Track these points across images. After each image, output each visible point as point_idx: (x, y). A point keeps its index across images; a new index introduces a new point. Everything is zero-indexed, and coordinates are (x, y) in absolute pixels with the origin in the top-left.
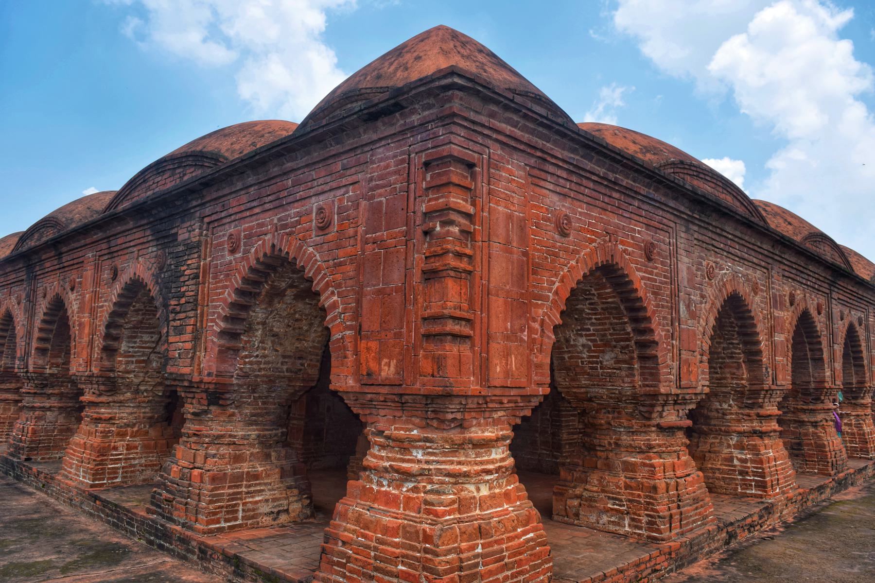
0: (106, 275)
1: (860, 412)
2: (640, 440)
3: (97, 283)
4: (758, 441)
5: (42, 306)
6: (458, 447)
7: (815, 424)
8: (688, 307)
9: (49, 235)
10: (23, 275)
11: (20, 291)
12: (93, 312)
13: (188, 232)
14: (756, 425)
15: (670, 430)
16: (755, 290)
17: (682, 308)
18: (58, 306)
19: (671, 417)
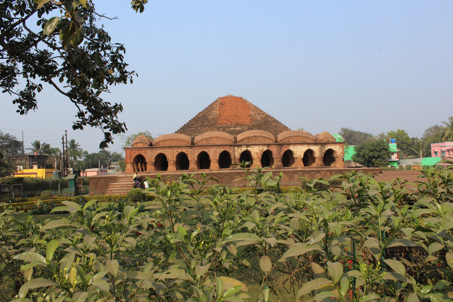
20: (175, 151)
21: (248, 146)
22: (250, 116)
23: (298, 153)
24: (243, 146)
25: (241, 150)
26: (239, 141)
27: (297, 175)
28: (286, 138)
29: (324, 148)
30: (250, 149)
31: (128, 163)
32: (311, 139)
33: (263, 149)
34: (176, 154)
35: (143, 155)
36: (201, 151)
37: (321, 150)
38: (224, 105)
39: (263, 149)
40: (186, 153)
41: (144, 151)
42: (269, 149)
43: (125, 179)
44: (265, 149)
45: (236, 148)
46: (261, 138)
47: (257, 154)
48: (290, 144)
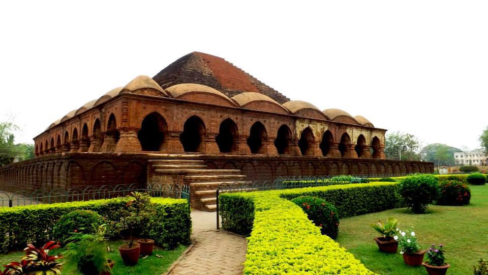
1: (268, 143)
3: (92, 119)
4: (207, 143)
5: (83, 125)
6: (127, 134)
8: (176, 118)
10: (78, 120)
11: (79, 123)
12: (92, 124)
13: (103, 110)
14: (208, 140)
15: (173, 137)
16: (204, 114)
17: (175, 118)
18: (86, 125)
19: (173, 134)
20: (219, 114)
21: (311, 121)
22: (253, 84)
24: (306, 121)
25: (303, 126)
26: (295, 113)
28: (337, 117)
29: (372, 135)
30: (311, 126)
31: (130, 129)
32: (357, 123)
33: (324, 128)
34: (220, 121)
35: (163, 114)
36: (255, 120)
37: (370, 138)
38: (210, 63)
39: (324, 128)
41: (163, 107)
42: (330, 130)
43: (174, 163)
46: (315, 113)
47: (318, 134)
48: (347, 125)
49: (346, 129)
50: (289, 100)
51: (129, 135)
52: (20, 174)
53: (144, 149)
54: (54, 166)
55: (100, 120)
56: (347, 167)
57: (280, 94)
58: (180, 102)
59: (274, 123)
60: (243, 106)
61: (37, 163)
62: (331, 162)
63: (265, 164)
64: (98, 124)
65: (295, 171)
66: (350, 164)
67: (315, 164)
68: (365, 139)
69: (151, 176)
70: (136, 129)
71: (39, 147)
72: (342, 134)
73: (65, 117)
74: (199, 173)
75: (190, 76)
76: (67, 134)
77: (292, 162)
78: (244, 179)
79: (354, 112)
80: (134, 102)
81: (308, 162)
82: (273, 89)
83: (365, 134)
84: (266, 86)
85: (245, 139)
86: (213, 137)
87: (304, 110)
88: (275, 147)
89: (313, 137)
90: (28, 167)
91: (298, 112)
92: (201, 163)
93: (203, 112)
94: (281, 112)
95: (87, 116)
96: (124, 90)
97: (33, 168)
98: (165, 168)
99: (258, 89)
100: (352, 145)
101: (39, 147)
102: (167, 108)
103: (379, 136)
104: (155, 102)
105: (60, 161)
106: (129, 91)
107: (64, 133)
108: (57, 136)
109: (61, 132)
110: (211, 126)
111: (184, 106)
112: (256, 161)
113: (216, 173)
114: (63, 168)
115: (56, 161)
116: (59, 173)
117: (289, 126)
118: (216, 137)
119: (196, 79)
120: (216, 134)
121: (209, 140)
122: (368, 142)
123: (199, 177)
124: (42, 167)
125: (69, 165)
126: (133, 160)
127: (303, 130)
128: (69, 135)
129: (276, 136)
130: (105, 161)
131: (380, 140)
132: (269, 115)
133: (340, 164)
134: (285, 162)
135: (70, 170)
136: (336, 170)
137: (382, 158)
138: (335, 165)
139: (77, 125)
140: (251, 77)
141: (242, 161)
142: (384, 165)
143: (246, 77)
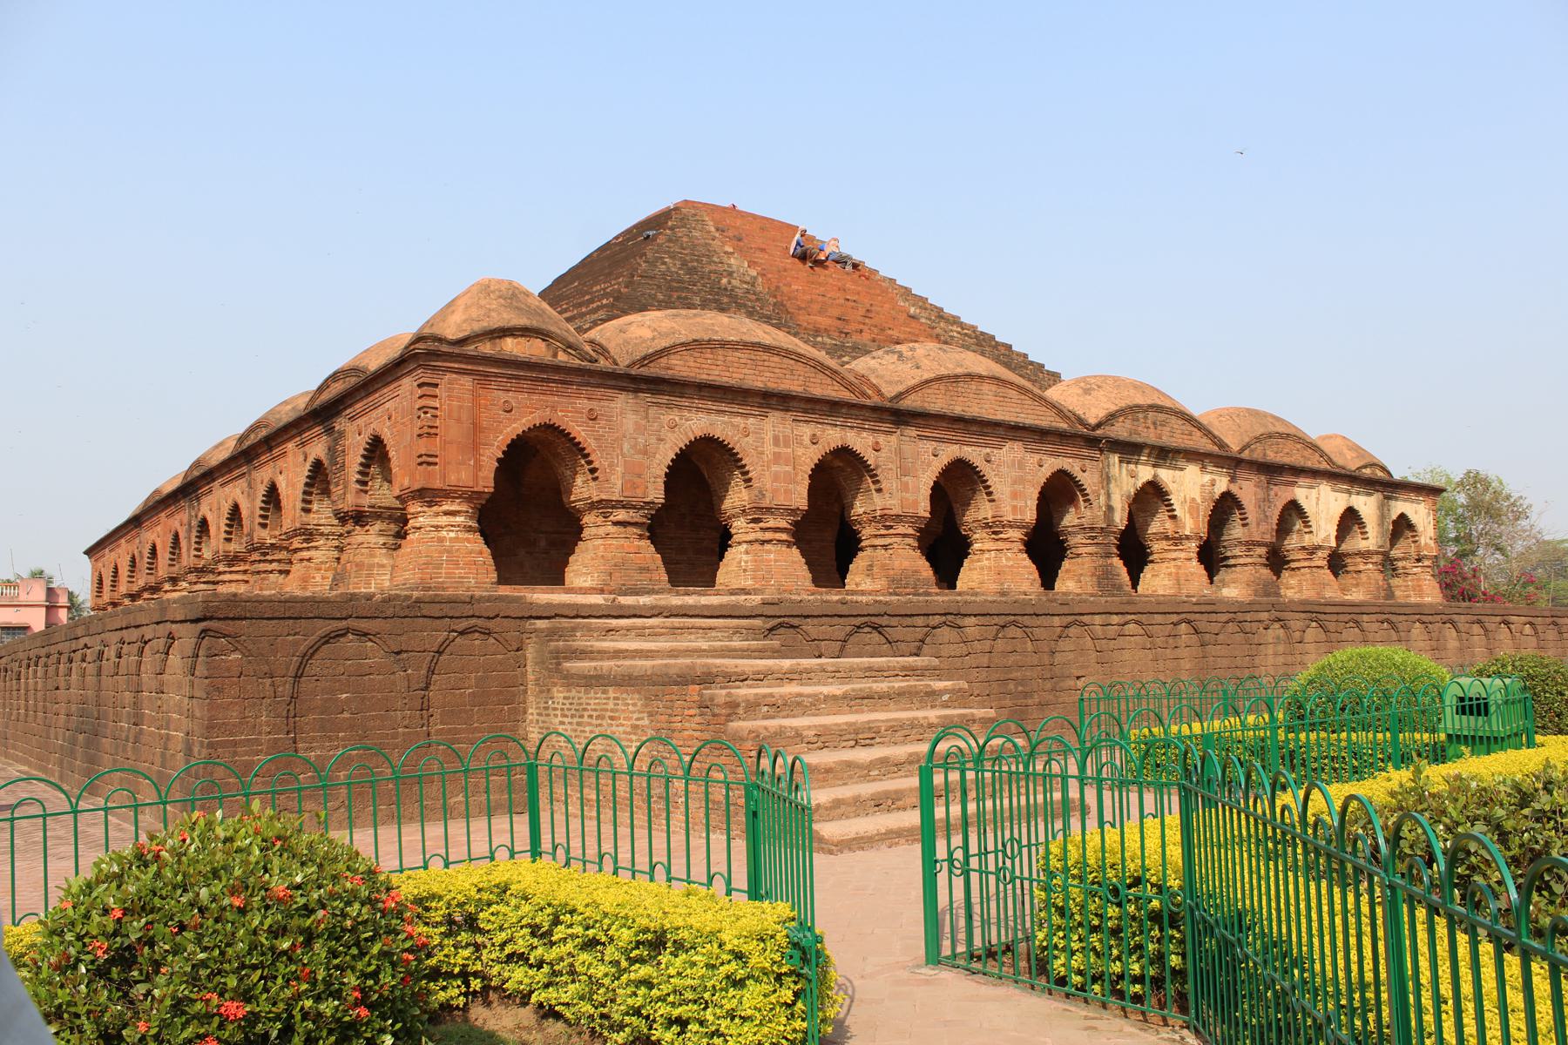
0: (302, 458)
1: (1000, 545)
2: (602, 531)
4: (757, 546)
5: (261, 490)
6: (437, 514)
7: (885, 547)
8: (634, 447)
9: (263, 433)
11: (242, 483)
13: (341, 424)
14: (760, 536)
17: (626, 446)
19: (621, 515)
20: (806, 431)
21: (1164, 455)
23: (1322, 523)
26: (1099, 425)
27: (1454, 633)
28: (1258, 439)
30: (1165, 475)
31: (446, 494)
32: (1330, 461)
34: (809, 457)
35: (580, 432)
37: (1382, 517)
40: (871, 458)
41: (583, 404)
43: (641, 633)
44: (1222, 484)
45: (1115, 458)
46: (1175, 422)
48: (1298, 471)
49: (1293, 484)
50: (1055, 377)
51: (444, 520)
52: (27, 684)
53: (503, 580)
54: (141, 652)
55: (326, 463)
56: (1322, 636)
57: (1018, 354)
58: (648, 382)
59: (1021, 465)
60: (900, 396)
61: (82, 642)
62: (1264, 616)
63: (1013, 631)
64: (319, 478)
65: (1126, 655)
66: (1331, 626)
67: (1202, 626)
68: (1362, 525)
69: (545, 691)
70: (470, 496)
71: (107, 582)
72: (1280, 505)
73: (197, 464)
74: (761, 677)
75: (672, 289)
76: (204, 524)
77: (1115, 619)
78: (960, 698)
79: (1322, 415)
80: (467, 381)
81: (1175, 618)
82: (993, 338)
83: (1367, 505)
84: (962, 325)
85: (911, 531)
86: (783, 524)
87: (1132, 410)
88: (1028, 562)
89: (1174, 517)
90: (54, 658)
91: (1111, 417)
92: (753, 633)
93: (738, 420)
94: (1047, 420)
95: (276, 452)
96: (419, 338)
97: (71, 661)
98: (603, 654)
99: (938, 336)
100: (1319, 547)
101: (107, 582)
102: (594, 404)
103: (1418, 512)
104: (548, 381)
105: (163, 630)
106: (440, 340)
107: (194, 523)
108: (170, 538)
109: (179, 520)
110: (776, 478)
111: (664, 399)
112: (973, 620)
113: (836, 675)
114: (175, 659)
115: (148, 632)
116: (162, 684)
117: (1080, 476)
118: (796, 524)
119: (697, 300)
120: (793, 512)
121: (768, 536)
122: (1371, 538)
123: (771, 695)
124: (101, 654)
125: (198, 646)
126: (463, 624)
127: (1132, 491)
128: (213, 530)
129: (1030, 515)
130: (348, 630)
131: (1420, 528)
132: (1001, 431)
133: (1296, 623)
134: (1085, 619)
135: (201, 670)
136: (1281, 648)
137: (1428, 599)
138: (1276, 631)
139: (238, 491)
140: (907, 292)
141: (920, 621)
142: (1452, 622)
143: (885, 291)
